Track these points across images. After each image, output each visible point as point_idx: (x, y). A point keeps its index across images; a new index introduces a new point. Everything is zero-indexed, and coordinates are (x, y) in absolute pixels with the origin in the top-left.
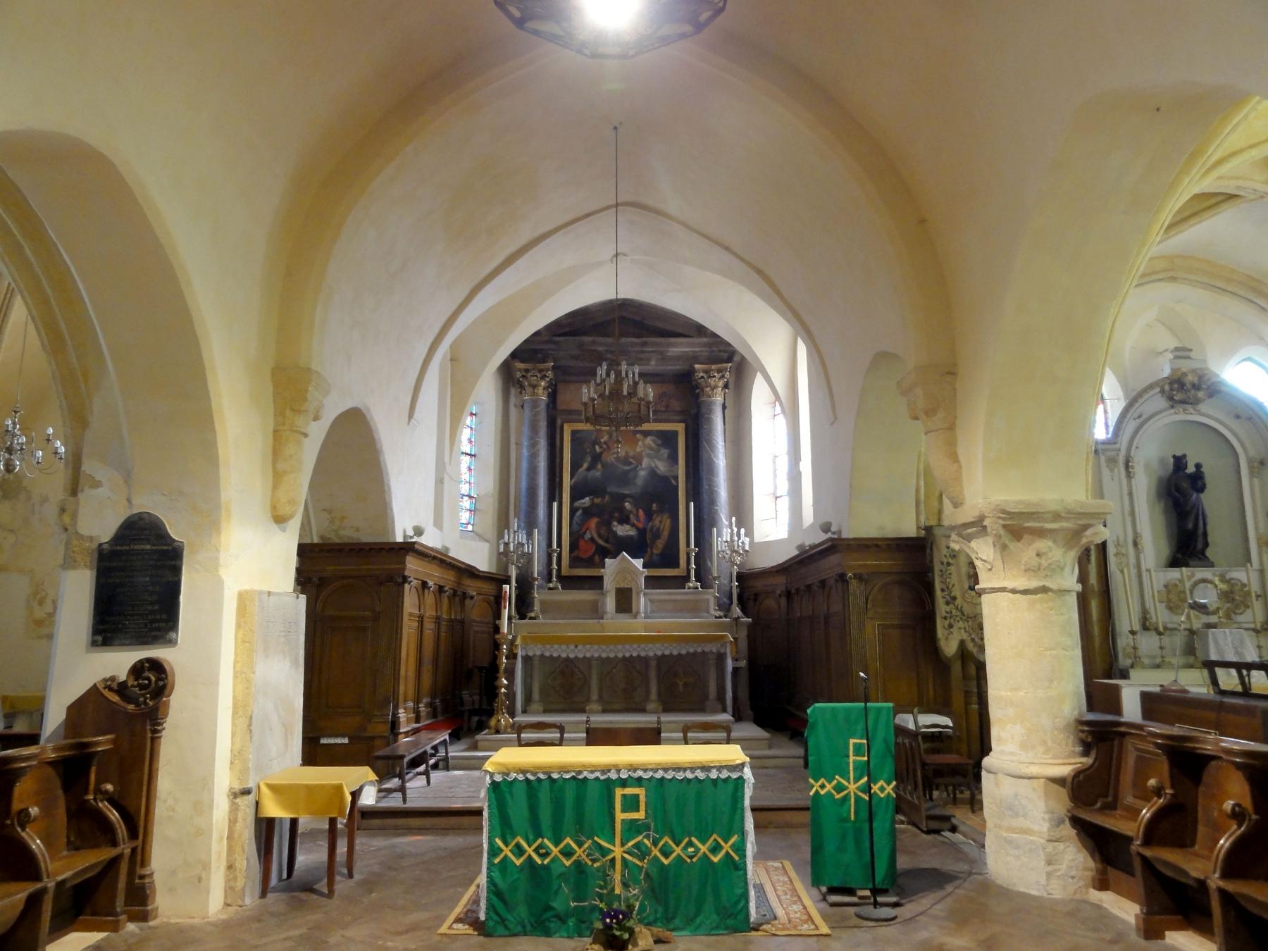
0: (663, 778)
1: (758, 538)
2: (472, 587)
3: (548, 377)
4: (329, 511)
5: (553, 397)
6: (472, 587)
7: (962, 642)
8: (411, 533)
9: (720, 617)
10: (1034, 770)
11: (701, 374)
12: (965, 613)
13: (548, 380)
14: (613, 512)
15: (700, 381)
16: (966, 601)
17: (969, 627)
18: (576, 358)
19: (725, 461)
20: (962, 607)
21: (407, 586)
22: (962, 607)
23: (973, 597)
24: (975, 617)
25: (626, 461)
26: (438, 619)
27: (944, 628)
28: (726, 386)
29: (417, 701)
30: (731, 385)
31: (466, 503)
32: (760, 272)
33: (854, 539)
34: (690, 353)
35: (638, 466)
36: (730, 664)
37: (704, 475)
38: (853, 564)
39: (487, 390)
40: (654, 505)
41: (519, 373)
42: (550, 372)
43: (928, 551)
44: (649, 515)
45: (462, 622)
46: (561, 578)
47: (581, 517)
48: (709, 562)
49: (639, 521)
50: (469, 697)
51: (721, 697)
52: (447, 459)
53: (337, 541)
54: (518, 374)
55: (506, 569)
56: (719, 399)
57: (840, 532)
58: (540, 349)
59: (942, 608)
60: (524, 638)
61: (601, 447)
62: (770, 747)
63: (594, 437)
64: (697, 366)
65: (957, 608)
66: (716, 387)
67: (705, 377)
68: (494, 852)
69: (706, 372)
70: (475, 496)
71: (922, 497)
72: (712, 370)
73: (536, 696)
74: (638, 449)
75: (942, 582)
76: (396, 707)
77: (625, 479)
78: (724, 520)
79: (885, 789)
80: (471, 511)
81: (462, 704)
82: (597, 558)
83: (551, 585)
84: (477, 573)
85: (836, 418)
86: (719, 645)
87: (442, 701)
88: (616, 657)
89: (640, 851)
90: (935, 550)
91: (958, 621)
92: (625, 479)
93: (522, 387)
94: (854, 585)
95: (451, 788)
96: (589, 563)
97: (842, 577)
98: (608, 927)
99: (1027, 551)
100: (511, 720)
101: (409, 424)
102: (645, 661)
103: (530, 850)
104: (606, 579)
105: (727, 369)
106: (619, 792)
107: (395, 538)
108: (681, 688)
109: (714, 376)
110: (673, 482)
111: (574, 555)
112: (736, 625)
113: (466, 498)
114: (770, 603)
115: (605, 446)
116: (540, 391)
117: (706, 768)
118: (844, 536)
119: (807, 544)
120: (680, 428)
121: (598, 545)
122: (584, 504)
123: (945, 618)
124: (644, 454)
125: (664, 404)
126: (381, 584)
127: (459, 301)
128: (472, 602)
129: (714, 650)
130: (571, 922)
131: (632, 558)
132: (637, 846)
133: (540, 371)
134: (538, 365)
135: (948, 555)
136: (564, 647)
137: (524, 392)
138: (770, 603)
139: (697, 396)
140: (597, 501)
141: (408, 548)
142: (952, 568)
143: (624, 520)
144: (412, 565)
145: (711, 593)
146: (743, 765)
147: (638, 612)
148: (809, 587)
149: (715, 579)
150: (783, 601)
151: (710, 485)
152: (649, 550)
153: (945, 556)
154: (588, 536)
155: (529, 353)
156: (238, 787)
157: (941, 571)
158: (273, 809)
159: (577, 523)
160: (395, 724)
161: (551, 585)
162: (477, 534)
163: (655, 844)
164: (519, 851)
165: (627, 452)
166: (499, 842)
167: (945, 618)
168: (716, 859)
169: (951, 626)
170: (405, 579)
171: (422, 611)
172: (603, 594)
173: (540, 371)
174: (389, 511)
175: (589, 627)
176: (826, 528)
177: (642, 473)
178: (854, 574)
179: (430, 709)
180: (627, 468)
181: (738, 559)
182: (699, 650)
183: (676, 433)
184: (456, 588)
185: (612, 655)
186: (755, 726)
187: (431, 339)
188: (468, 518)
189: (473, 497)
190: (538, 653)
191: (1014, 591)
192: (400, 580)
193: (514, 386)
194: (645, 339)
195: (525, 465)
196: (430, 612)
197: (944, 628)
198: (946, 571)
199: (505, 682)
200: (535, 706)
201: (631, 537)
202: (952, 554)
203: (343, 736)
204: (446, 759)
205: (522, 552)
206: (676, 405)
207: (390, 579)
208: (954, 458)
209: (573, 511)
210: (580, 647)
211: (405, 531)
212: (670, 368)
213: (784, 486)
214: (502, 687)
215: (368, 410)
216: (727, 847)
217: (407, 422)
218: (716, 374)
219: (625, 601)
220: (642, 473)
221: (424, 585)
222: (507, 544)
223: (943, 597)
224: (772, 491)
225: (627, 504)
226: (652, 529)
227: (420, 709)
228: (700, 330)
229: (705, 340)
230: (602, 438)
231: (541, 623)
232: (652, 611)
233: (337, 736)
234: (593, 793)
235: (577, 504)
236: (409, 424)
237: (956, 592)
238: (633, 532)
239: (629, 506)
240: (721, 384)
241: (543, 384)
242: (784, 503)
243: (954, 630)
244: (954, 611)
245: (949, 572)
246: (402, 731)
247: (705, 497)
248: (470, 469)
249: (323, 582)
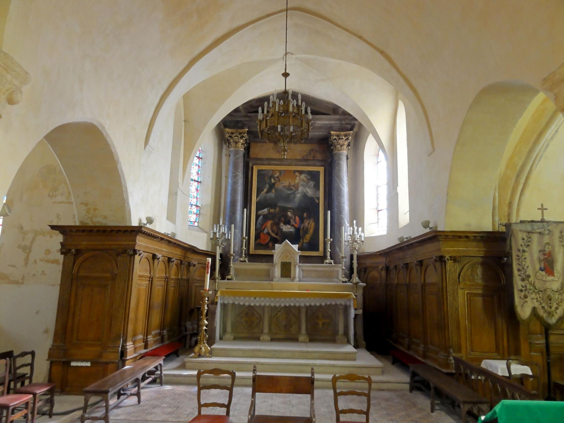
1: (367, 235)
2: (194, 259)
3: (244, 137)
4: (86, 205)
5: (248, 149)
6: (194, 259)
7: (534, 309)
8: (145, 221)
9: (346, 282)
11: (335, 137)
12: (537, 287)
13: (244, 139)
15: (333, 141)
16: (538, 279)
17: (540, 298)
19: (347, 189)
20: (534, 283)
21: (137, 257)
22: (534, 283)
23: (543, 276)
24: (545, 290)
25: (289, 188)
26: (167, 279)
27: (520, 298)
28: (349, 145)
29: (147, 333)
30: (352, 144)
31: (194, 209)
32: (382, 53)
33: (452, 232)
34: (329, 125)
35: (295, 192)
36: (352, 313)
37: (335, 198)
40: (305, 214)
41: (227, 134)
42: (245, 134)
43: (508, 241)
44: (302, 220)
45: (188, 280)
47: (263, 220)
48: (338, 249)
49: (296, 223)
51: (346, 333)
52: (180, 180)
53: (91, 224)
54: (227, 135)
56: (345, 152)
57: (436, 227)
58: (241, 121)
59: (518, 283)
60: (222, 293)
61: (275, 180)
62: (383, 373)
63: (271, 174)
64: (332, 132)
65: (531, 284)
67: (337, 139)
69: (338, 136)
70: (200, 206)
71: (497, 204)
72: (341, 135)
73: (229, 328)
74: (296, 181)
75: (519, 264)
76: (125, 341)
77: (288, 199)
78: (347, 224)
80: (197, 214)
81: (186, 330)
82: (271, 244)
83: (242, 259)
84: (198, 251)
85: (434, 150)
86: (346, 301)
87: (168, 331)
88: (280, 305)
90: (512, 239)
91: (532, 293)
92: (288, 199)
94: (449, 264)
95: (154, 408)
100: (209, 348)
101: (145, 149)
102: (299, 308)
105: (350, 134)
107: (131, 223)
108: (320, 326)
109: (343, 139)
110: (317, 201)
111: (257, 242)
112: (356, 287)
113: (194, 207)
115: (277, 179)
116: (240, 145)
118: (439, 229)
119: (405, 237)
120: (321, 169)
121: (271, 237)
122: (264, 212)
123: (521, 291)
124: (299, 184)
125: (312, 155)
126: (118, 255)
127: (181, 68)
128: (195, 268)
129: (343, 303)
131: (292, 244)
133: (240, 133)
134: (239, 130)
135: (523, 244)
136: (247, 299)
137: (230, 146)
138: (375, 274)
139: (332, 150)
140: (272, 211)
141: (138, 230)
142: (527, 255)
143: (287, 222)
144: (141, 242)
145: (340, 267)
147: (295, 278)
148: (407, 265)
149: (343, 258)
150: (383, 273)
151: (338, 203)
152: (301, 241)
153: (521, 245)
154: (266, 231)
157: (518, 256)
159: (260, 223)
160: (123, 354)
162: (200, 228)
165: (290, 183)
167: (521, 291)
169: (526, 297)
170: (135, 252)
171: (152, 274)
172: (273, 266)
173: (240, 133)
174: (126, 205)
175: (263, 286)
176: (426, 225)
177: (298, 195)
178: (450, 257)
179: (158, 337)
180: (289, 192)
182: (333, 303)
183: (318, 173)
184: (182, 260)
185: (278, 305)
186: (366, 351)
187: (161, 93)
188: (195, 218)
189: (199, 206)
190: (231, 302)
192: (131, 252)
193: (225, 143)
195: (229, 188)
197: (520, 298)
198: (522, 256)
199: (206, 322)
200: (228, 336)
201: (291, 232)
202: (526, 244)
203: (86, 361)
204: (160, 377)
205: (225, 238)
206: (319, 156)
209: (257, 217)
210: (257, 299)
211: (140, 220)
213: (384, 204)
214: (204, 325)
215: (104, 128)
217: (144, 147)
218: (344, 137)
220: (298, 195)
221: (154, 257)
223: (519, 275)
224: (376, 207)
225: (289, 213)
226: (303, 228)
227: (148, 339)
228: (335, 110)
229: (338, 117)
230: (275, 175)
232: (303, 277)
233: (83, 361)
235: (260, 212)
236: (145, 149)
237: (530, 272)
238: (292, 230)
239: (291, 215)
240: (346, 143)
241: (242, 141)
242: (384, 216)
243: (528, 299)
244: (528, 286)
245: (524, 257)
246: (128, 358)
247: (336, 209)
248: (197, 190)
249: (78, 252)
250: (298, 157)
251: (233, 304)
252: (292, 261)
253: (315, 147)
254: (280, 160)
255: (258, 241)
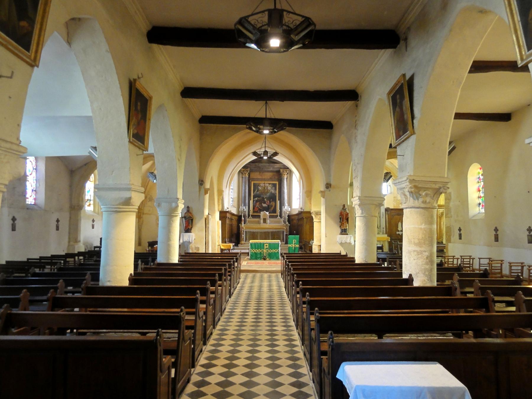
0: (270, 243)
2: (234, 218)
5: (249, 176)
6: (234, 218)
10: (317, 244)
11: (282, 172)
14: (262, 201)
18: (255, 168)
28: (287, 174)
30: (289, 173)
31: (231, 200)
37: (282, 194)
38: (304, 216)
39: (236, 177)
44: (270, 202)
46: (252, 216)
47: (255, 203)
50: (233, 239)
55: (242, 214)
56: (286, 177)
57: (303, 210)
60: (245, 228)
66: (285, 174)
68: (251, 251)
69: (283, 171)
73: (248, 239)
76: (226, 239)
78: (286, 204)
79: (298, 246)
82: (259, 211)
89: (267, 251)
93: (242, 173)
94: (305, 220)
96: (257, 212)
97: (303, 218)
98: (264, 258)
99: (318, 217)
102: (268, 232)
103: (255, 251)
104: (261, 216)
106: (265, 245)
114: (295, 221)
116: (247, 175)
117: (275, 242)
120: (277, 183)
130: (260, 258)
132: (267, 250)
133: (247, 170)
138: (295, 221)
139: (281, 176)
140: (259, 199)
141: (228, 212)
143: (265, 203)
144: (228, 215)
146: (279, 242)
147: (267, 223)
150: (297, 221)
152: (270, 210)
154: (257, 206)
155: (245, 167)
156: (218, 245)
158: (222, 248)
161: (250, 217)
163: (269, 250)
164: (254, 251)
166: (251, 250)
168: (276, 252)
170: (227, 217)
176: (301, 209)
181: (288, 213)
182: (279, 230)
183: (276, 184)
185: (262, 231)
190: (248, 231)
191: (317, 222)
194: (269, 164)
195: (243, 191)
196: (229, 223)
199: (243, 235)
201: (266, 207)
206: (276, 177)
207: (224, 217)
208: (311, 204)
209: (253, 201)
212: (275, 170)
216: (277, 251)
219: (265, 221)
221: (228, 218)
222: (241, 209)
228: (282, 163)
231: (248, 224)
234: (262, 245)
235: (254, 199)
240: (286, 174)
242: (299, 200)
247: (282, 199)
250: (269, 178)
251: (249, 231)
252: (267, 218)
253: (275, 173)
254: (262, 179)
255: (254, 210)
